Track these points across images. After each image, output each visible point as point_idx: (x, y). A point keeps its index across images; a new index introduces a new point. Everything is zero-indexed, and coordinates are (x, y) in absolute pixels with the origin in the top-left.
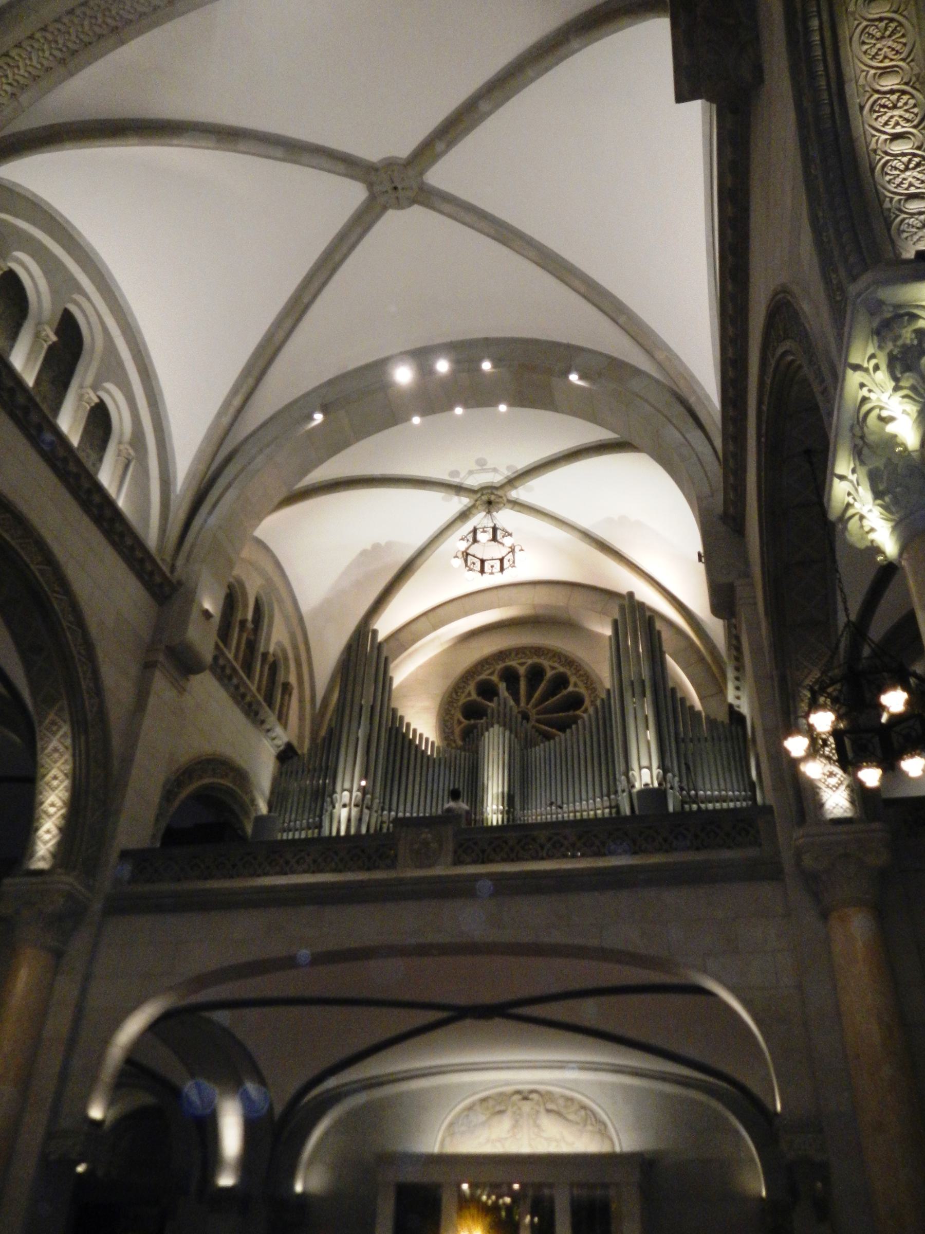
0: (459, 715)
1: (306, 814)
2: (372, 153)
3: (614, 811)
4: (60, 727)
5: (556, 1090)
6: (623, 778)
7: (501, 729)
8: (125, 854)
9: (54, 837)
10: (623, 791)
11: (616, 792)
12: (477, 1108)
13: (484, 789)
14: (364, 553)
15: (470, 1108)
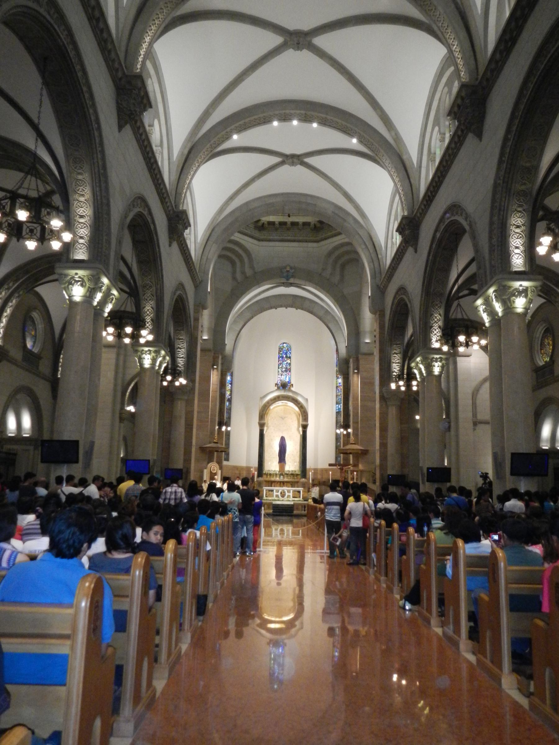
2: (288, 152)
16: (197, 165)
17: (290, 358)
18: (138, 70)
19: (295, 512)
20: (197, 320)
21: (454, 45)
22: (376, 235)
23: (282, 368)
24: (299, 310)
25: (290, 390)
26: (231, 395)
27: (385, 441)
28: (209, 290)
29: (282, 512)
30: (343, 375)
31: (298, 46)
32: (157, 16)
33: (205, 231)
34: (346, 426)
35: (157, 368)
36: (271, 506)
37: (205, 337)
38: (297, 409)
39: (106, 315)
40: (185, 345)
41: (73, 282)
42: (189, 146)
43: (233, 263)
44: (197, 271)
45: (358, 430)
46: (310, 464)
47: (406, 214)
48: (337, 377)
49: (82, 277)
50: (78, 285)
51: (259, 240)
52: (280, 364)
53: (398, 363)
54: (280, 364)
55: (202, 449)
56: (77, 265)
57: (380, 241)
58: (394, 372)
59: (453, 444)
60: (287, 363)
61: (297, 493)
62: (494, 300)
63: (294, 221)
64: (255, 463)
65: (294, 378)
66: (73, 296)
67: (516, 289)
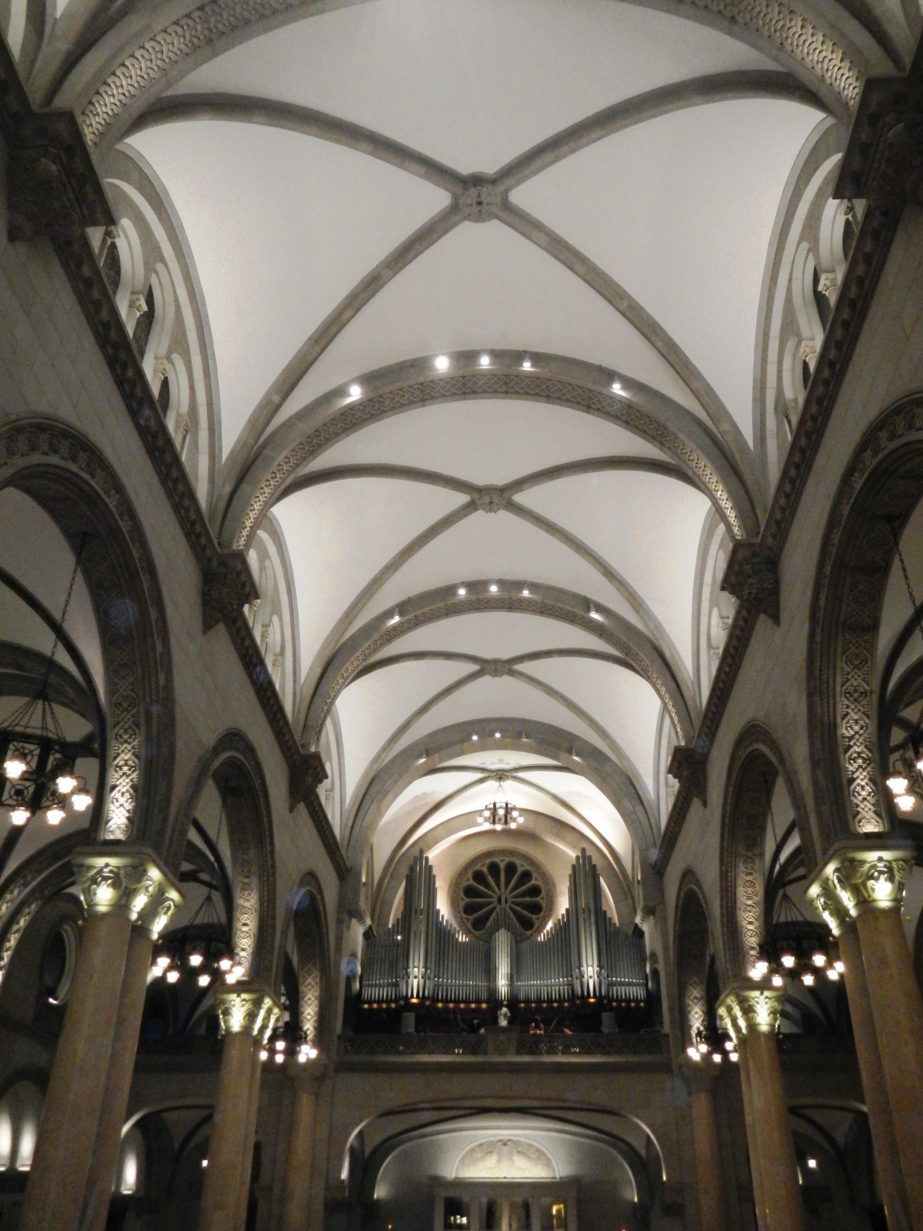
0: (462, 895)
1: (386, 977)
2: (488, 656)
3: (570, 987)
4: (313, 972)
5: (522, 1139)
6: (577, 970)
7: (506, 931)
8: (339, 1037)
9: (312, 1032)
10: (577, 978)
11: (572, 976)
12: (477, 1149)
13: (495, 970)
14: (417, 797)
15: (473, 1150)
16: (341, 681)
18: (241, 547)
20: (339, 939)
21: (718, 491)
31: (491, 507)
32: (273, 475)
35: (255, 1032)
39: (155, 936)
41: (100, 879)
42: (328, 653)
47: (683, 743)
49: (115, 870)
50: (108, 886)
56: (109, 849)
62: (838, 886)
66: (95, 905)
67: (874, 867)
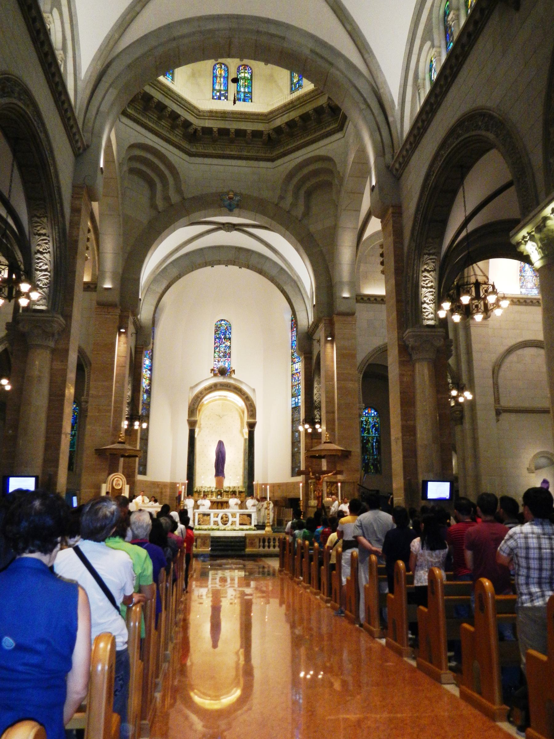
17: (230, 339)
19: (249, 550)
20: (76, 211)
22: (385, 82)
23: (219, 352)
24: (244, 269)
25: (230, 377)
26: (150, 384)
27: (411, 423)
28: (102, 165)
29: (227, 550)
30: (304, 354)
33: (93, 60)
34: (310, 420)
36: (208, 542)
37: (108, 285)
38: (240, 402)
40: (50, 246)
43: (151, 185)
44: (80, 126)
45: (334, 425)
46: (258, 479)
48: (292, 361)
51: (190, 154)
52: (217, 347)
53: (431, 287)
54: (217, 347)
55: (100, 453)
57: (390, 92)
58: (425, 302)
59: (469, 442)
60: (226, 347)
61: (245, 517)
63: (239, 128)
64: (182, 478)
65: (234, 363)
